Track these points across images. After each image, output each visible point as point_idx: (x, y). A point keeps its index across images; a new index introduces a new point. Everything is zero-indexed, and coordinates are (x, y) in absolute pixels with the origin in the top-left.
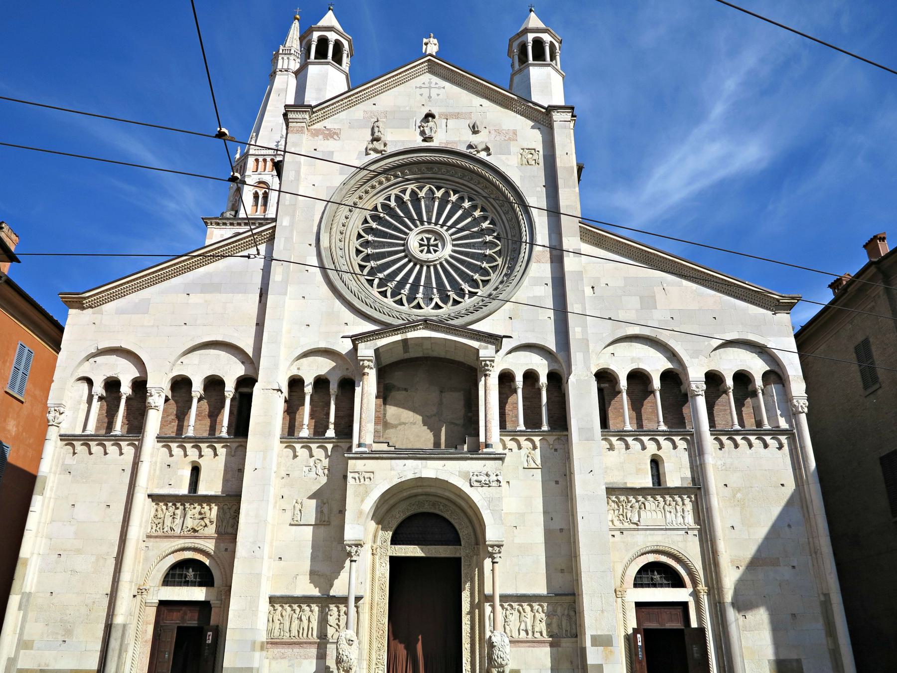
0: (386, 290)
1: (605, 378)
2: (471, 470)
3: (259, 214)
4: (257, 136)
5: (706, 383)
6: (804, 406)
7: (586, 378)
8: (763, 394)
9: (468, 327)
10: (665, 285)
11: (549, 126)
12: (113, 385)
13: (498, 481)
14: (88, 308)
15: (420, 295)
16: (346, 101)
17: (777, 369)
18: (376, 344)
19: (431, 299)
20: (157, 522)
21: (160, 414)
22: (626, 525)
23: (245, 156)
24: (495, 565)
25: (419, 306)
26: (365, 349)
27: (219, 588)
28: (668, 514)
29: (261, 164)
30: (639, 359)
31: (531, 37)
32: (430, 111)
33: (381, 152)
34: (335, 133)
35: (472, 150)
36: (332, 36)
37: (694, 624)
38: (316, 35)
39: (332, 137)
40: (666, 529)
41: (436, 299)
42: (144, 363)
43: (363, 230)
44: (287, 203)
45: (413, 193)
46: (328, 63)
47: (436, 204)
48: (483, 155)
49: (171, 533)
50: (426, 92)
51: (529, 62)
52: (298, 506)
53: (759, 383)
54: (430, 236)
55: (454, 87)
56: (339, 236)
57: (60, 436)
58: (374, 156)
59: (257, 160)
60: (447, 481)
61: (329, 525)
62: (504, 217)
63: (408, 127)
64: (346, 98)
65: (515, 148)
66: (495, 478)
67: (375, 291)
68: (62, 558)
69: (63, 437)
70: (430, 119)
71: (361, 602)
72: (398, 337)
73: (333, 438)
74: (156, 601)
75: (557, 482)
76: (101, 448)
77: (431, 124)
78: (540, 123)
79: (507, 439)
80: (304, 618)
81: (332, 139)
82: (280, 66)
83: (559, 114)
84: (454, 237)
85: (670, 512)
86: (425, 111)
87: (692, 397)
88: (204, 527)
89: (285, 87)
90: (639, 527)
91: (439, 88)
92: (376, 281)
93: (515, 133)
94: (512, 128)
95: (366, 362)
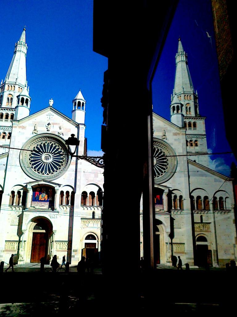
1: (84, 194)
4: (9, 77)
15: (44, 171)
23: (4, 84)
25: (43, 174)
29: (10, 87)
31: (77, 101)
36: (25, 98)
37: (97, 248)
38: (21, 97)
41: (48, 172)
48: (61, 136)
52: (12, 221)
56: (25, 155)
58: (34, 134)
63: (43, 127)
67: (33, 170)
71: (26, 242)
72: (37, 184)
77: (49, 126)
79: (61, 207)
82: (18, 49)
92: (34, 167)
93: (70, 129)
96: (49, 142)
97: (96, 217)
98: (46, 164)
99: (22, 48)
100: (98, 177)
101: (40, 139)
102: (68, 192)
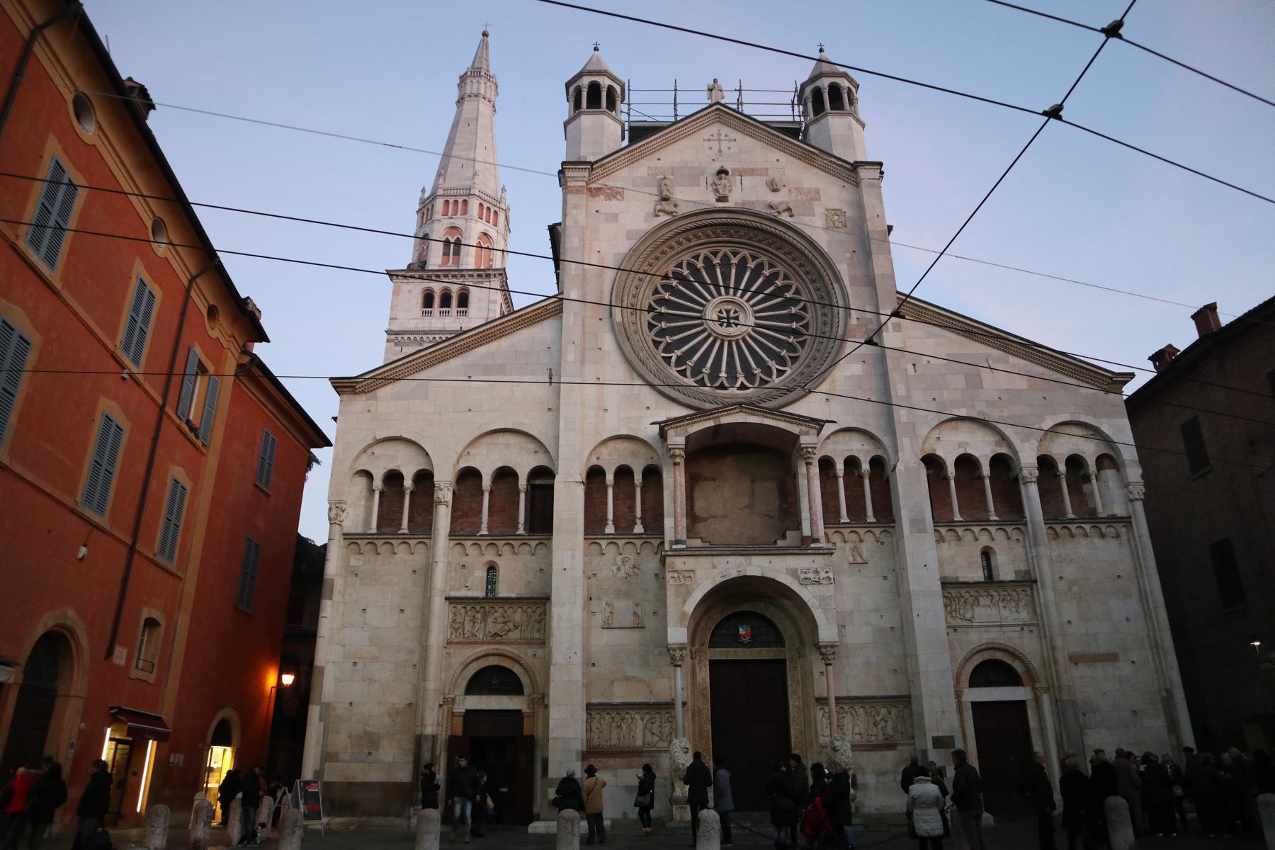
0: (686, 369)
1: (932, 462)
2: (799, 567)
3: (450, 265)
5: (1038, 469)
6: (1141, 492)
7: (915, 465)
8: (1096, 476)
9: (781, 410)
10: (991, 362)
11: (855, 184)
12: (394, 477)
13: (828, 577)
14: (360, 393)
15: (723, 374)
16: (628, 156)
17: (1111, 453)
18: (687, 431)
19: (736, 379)
20: (456, 626)
21: (450, 509)
22: (959, 622)
24: (830, 667)
25: (722, 387)
26: (676, 436)
27: (528, 696)
28: (1001, 608)
30: (966, 443)
32: (722, 166)
33: (672, 213)
34: (618, 193)
35: (773, 211)
39: (615, 197)
40: (1001, 626)
41: (741, 379)
42: (427, 454)
43: (654, 301)
44: (573, 272)
45: (707, 259)
46: (603, 113)
47: (733, 271)
48: (785, 217)
49: (473, 639)
50: (715, 145)
51: (828, 111)
53: (1092, 468)
54: (729, 307)
55: (747, 138)
57: (344, 534)
58: (664, 218)
59: (447, 202)
60: (774, 579)
61: (643, 628)
62: (810, 286)
64: (628, 153)
65: (819, 210)
66: (825, 575)
67: (673, 371)
68: (358, 667)
69: (346, 536)
70: (723, 175)
72: (711, 423)
73: (642, 534)
74: (464, 711)
75: (885, 578)
76: (387, 547)
77: (723, 182)
78: (844, 180)
79: (830, 532)
80: (624, 726)
81: (615, 199)
83: (866, 171)
84: (755, 308)
85: (1005, 607)
86: (717, 166)
87: (1024, 483)
88: (509, 631)
89: (476, 116)
90: (974, 624)
91: (730, 140)
92: (673, 360)
93: (817, 191)
94: (813, 186)
95: (677, 451)
96: (727, 250)
97: (1006, 570)
98: (730, 343)
99: (482, 86)
100: (984, 386)
101: (690, 235)
102: (851, 462)
